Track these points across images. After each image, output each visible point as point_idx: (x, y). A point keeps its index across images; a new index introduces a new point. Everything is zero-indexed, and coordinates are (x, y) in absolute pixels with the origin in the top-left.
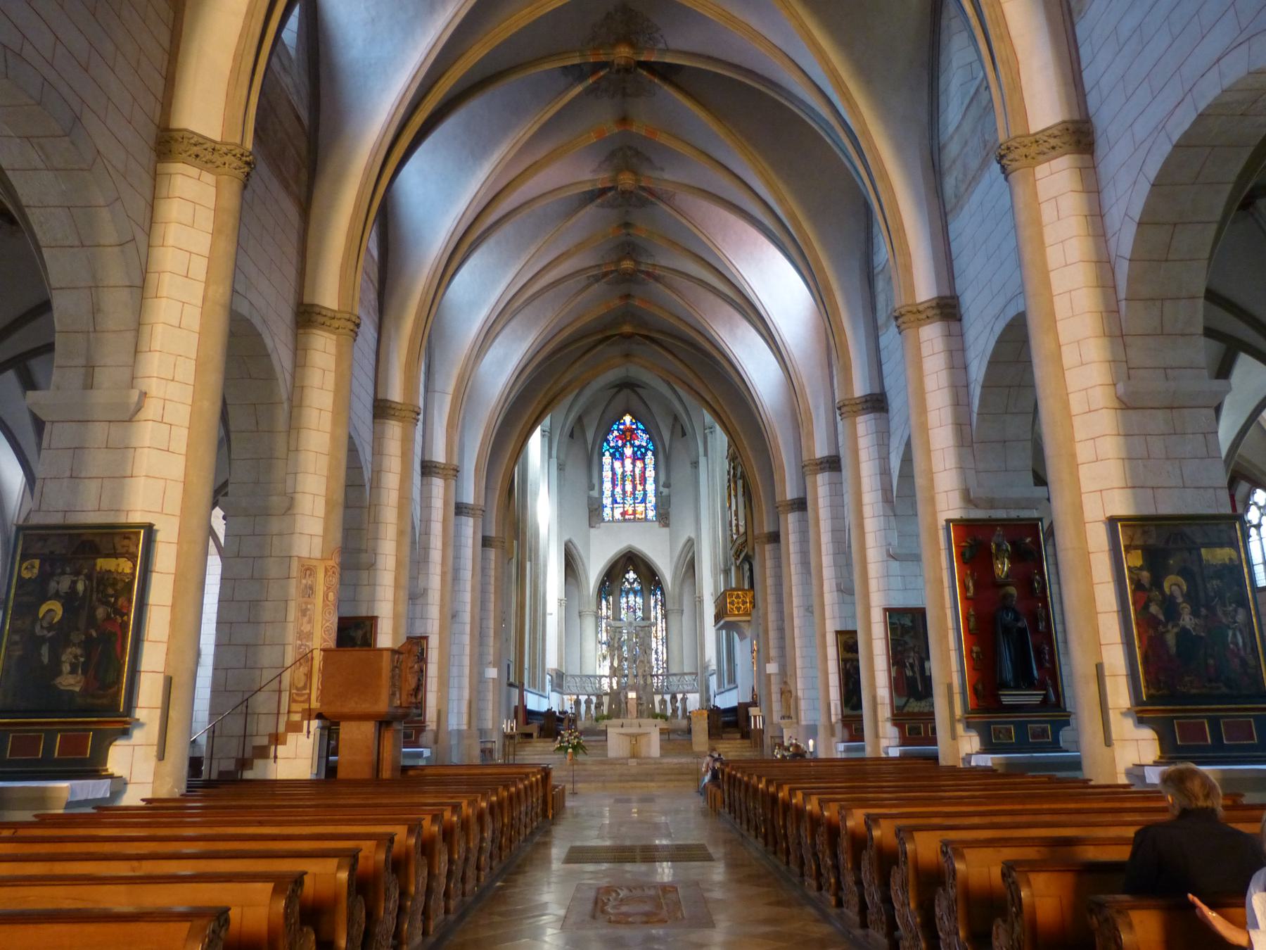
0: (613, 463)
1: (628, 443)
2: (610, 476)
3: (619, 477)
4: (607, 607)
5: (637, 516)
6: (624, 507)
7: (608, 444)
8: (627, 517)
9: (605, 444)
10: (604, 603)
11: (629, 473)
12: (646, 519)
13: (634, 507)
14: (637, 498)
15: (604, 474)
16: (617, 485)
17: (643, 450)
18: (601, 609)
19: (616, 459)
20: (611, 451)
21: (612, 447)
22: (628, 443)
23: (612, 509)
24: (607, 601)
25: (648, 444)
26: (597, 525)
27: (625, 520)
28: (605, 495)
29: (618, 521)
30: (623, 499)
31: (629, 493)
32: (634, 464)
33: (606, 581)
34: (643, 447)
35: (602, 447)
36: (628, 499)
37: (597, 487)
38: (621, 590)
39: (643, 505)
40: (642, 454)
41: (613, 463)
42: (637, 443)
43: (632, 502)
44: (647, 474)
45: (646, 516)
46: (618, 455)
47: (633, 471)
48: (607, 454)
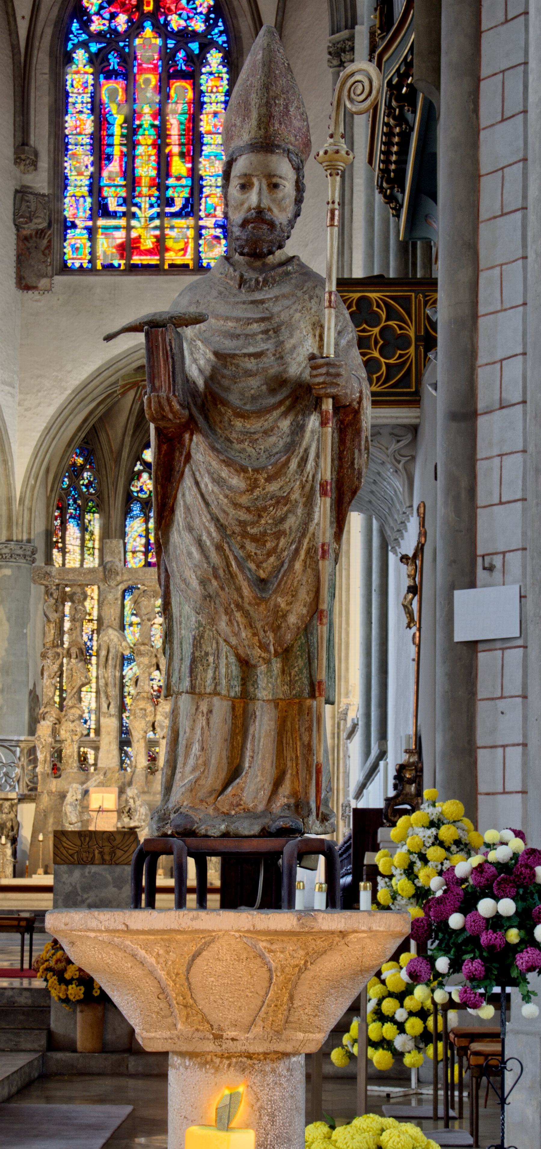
0: (97, 86)
1: (148, 24)
2: (89, 127)
3: (117, 130)
4: (83, 546)
5: (172, 257)
6: (129, 228)
7: (85, 25)
8: (136, 259)
9: (75, 26)
10: (73, 530)
11: (147, 121)
12: (200, 268)
13: (161, 228)
14: (170, 202)
15: (70, 121)
16: (109, 158)
17: (195, 47)
18: (63, 551)
19: (110, 75)
20: (94, 47)
21: (99, 36)
22: (148, 24)
23: (91, 232)
24: (84, 529)
25: (210, 28)
26: (43, 282)
27: (133, 269)
28: (71, 190)
29: (109, 267)
30: (128, 201)
31: (145, 181)
32: (163, 89)
33: (82, 468)
34: (194, 35)
35: (65, 34)
36: (144, 202)
37: (44, 163)
38: (129, 498)
39: (191, 221)
40: (190, 58)
41: (97, 86)
42: (176, 22)
43: (156, 210)
44: (206, 123)
45: (198, 258)
46: (114, 61)
47: (160, 113)
48: (80, 56)
